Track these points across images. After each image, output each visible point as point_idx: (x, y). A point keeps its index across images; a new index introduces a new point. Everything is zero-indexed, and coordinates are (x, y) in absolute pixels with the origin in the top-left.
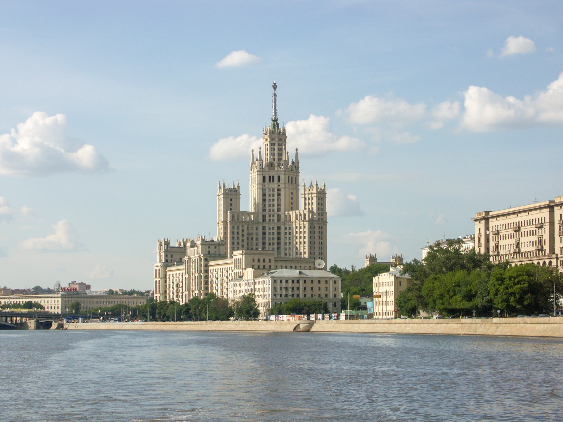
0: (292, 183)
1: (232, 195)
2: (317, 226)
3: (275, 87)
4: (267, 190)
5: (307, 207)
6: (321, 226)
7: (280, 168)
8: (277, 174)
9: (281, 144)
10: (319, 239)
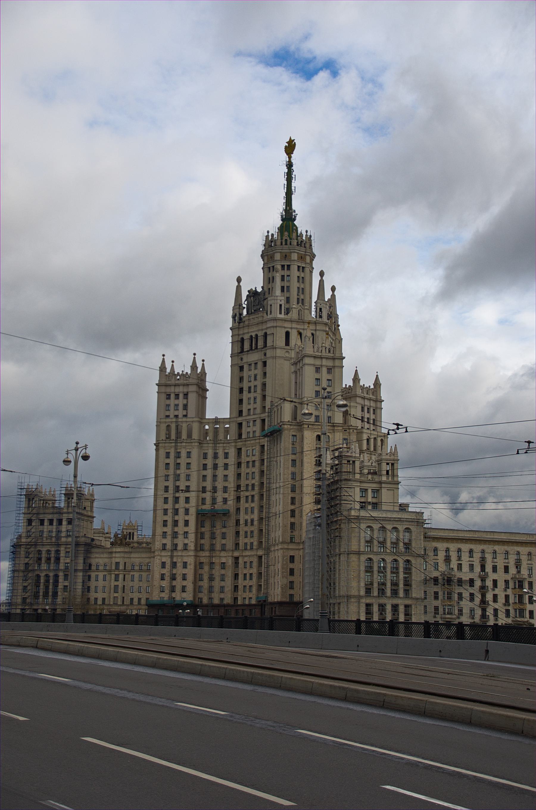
3: (290, 147)
4: (246, 368)
8: (262, 330)
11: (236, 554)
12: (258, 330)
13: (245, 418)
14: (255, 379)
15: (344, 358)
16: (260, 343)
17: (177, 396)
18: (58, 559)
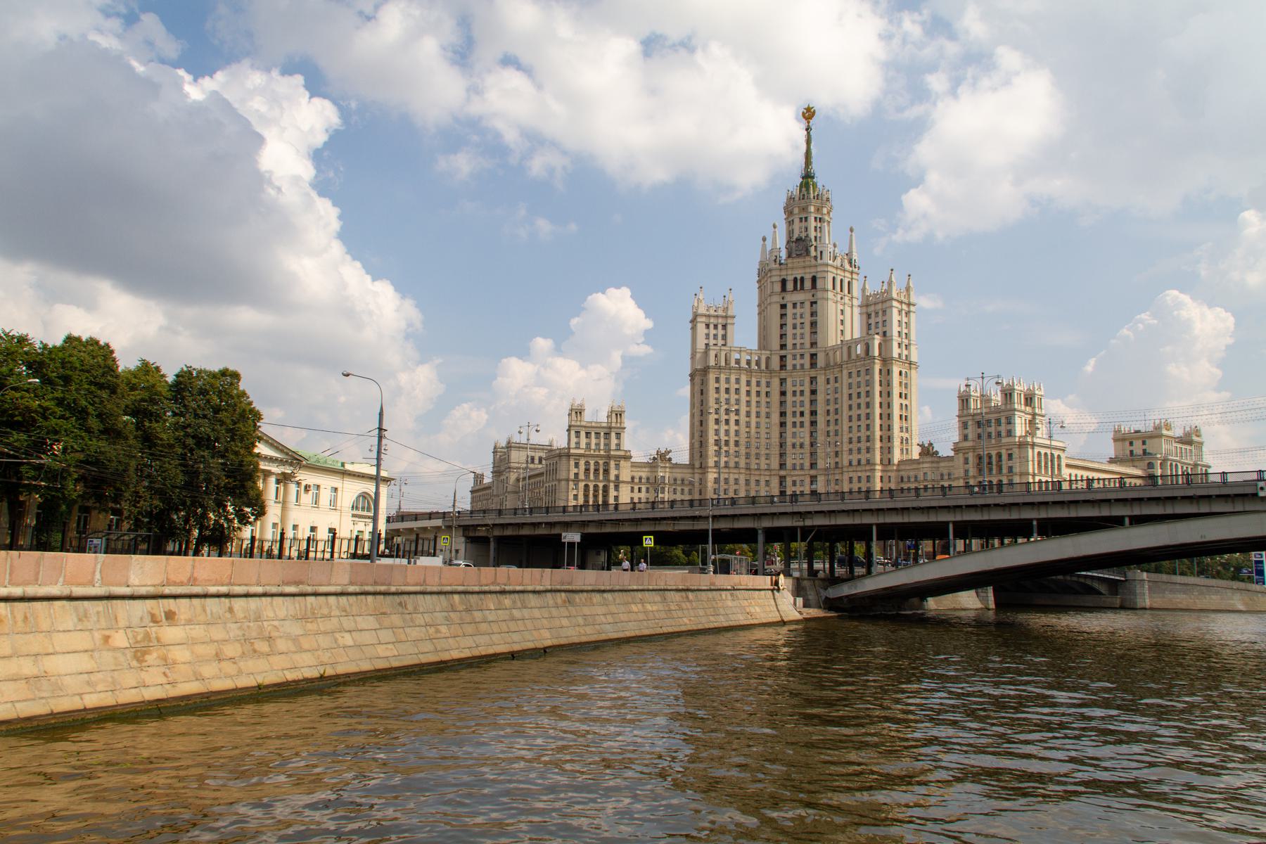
0: (841, 291)
1: (717, 317)
2: (896, 370)
4: (790, 306)
5: (871, 332)
6: (903, 372)
8: (810, 273)
9: (820, 219)
10: (901, 397)
11: (783, 473)
12: (805, 273)
14: (801, 317)
16: (808, 284)
17: (716, 327)
18: (606, 471)
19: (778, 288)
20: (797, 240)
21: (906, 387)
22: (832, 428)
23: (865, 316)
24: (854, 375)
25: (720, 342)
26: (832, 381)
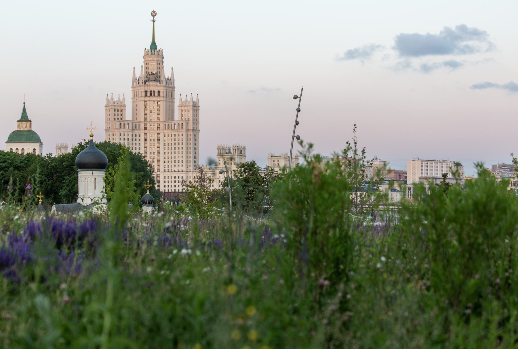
0: (169, 97)
1: (118, 106)
3: (154, 14)
7: (160, 84)
8: (157, 89)
9: (160, 63)
12: (155, 89)
13: (149, 122)
15: (200, 107)
16: (156, 94)
17: (118, 110)
19: (143, 94)
20: (152, 74)
21: (196, 141)
22: (166, 155)
23: (180, 111)
24: (177, 135)
25: (120, 117)
26: (166, 136)
